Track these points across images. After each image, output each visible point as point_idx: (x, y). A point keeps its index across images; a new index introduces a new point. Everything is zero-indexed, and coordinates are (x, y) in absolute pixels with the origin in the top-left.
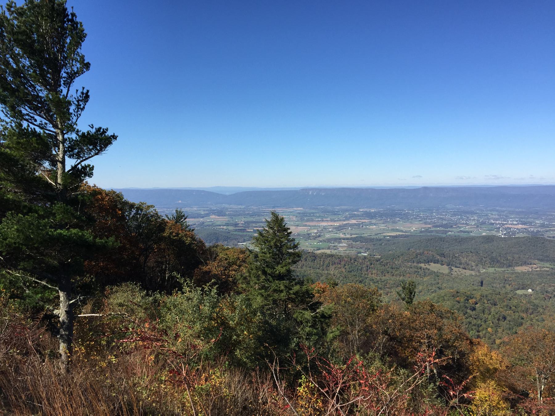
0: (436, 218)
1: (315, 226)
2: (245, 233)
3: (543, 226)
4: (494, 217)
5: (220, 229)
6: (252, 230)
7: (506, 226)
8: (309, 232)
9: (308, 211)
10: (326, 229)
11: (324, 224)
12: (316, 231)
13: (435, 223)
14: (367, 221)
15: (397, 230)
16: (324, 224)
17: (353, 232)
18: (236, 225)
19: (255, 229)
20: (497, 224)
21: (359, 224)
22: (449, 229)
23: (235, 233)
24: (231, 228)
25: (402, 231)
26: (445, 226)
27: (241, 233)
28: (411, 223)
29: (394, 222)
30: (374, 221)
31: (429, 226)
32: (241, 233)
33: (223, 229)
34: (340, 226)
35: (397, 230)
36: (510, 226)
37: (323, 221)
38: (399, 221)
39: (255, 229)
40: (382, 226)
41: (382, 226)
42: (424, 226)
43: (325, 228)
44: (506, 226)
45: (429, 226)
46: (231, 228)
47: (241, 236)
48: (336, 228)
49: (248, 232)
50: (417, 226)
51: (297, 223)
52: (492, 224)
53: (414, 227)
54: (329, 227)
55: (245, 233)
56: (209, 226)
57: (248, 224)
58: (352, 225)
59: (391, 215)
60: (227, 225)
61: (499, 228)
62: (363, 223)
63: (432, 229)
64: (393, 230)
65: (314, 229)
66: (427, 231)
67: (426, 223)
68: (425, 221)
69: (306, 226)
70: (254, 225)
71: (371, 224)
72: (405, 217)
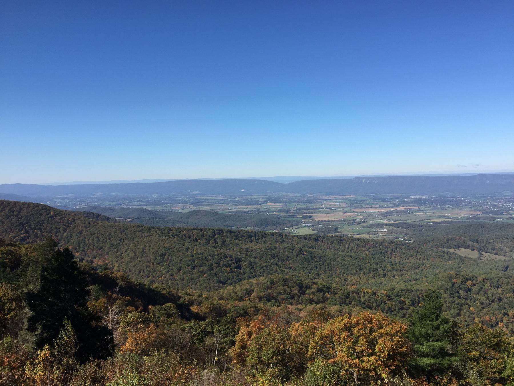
0: (489, 205)
1: (363, 212)
2: (294, 219)
5: (273, 215)
6: (301, 216)
8: (355, 218)
9: (359, 198)
10: (372, 215)
11: (372, 210)
12: (361, 217)
13: (485, 209)
14: (415, 208)
15: (444, 217)
16: (372, 210)
17: (399, 218)
18: (288, 211)
19: (305, 215)
21: (406, 211)
22: (499, 216)
23: (285, 219)
24: (283, 214)
25: (449, 218)
26: (496, 213)
27: (291, 219)
28: (461, 210)
30: (422, 208)
31: (479, 213)
32: (291, 219)
33: (275, 215)
34: (387, 213)
35: (444, 217)
37: (371, 208)
38: (449, 207)
39: (305, 215)
40: (430, 213)
41: (430, 213)
42: (473, 212)
43: (371, 214)
45: (479, 213)
46: (283, 214)
47: (290, 221)
48: (382, 214)
49: (298, 217)
50: (465, 213)
51: (345, 209)
53: (462, 214)
54: (376, 213)
55: (294, 219)
57: (299, 210)
58: (399, 212)
60: (280, 211)
62: (411, 209)
63: (481, 216)
64: (440, 217)
65: (361, 215)
66: (475, 217)
67: (476, 210)
68: (475, 208)
69: (354, 212)
70: (305, 211)
71: (419, 210)
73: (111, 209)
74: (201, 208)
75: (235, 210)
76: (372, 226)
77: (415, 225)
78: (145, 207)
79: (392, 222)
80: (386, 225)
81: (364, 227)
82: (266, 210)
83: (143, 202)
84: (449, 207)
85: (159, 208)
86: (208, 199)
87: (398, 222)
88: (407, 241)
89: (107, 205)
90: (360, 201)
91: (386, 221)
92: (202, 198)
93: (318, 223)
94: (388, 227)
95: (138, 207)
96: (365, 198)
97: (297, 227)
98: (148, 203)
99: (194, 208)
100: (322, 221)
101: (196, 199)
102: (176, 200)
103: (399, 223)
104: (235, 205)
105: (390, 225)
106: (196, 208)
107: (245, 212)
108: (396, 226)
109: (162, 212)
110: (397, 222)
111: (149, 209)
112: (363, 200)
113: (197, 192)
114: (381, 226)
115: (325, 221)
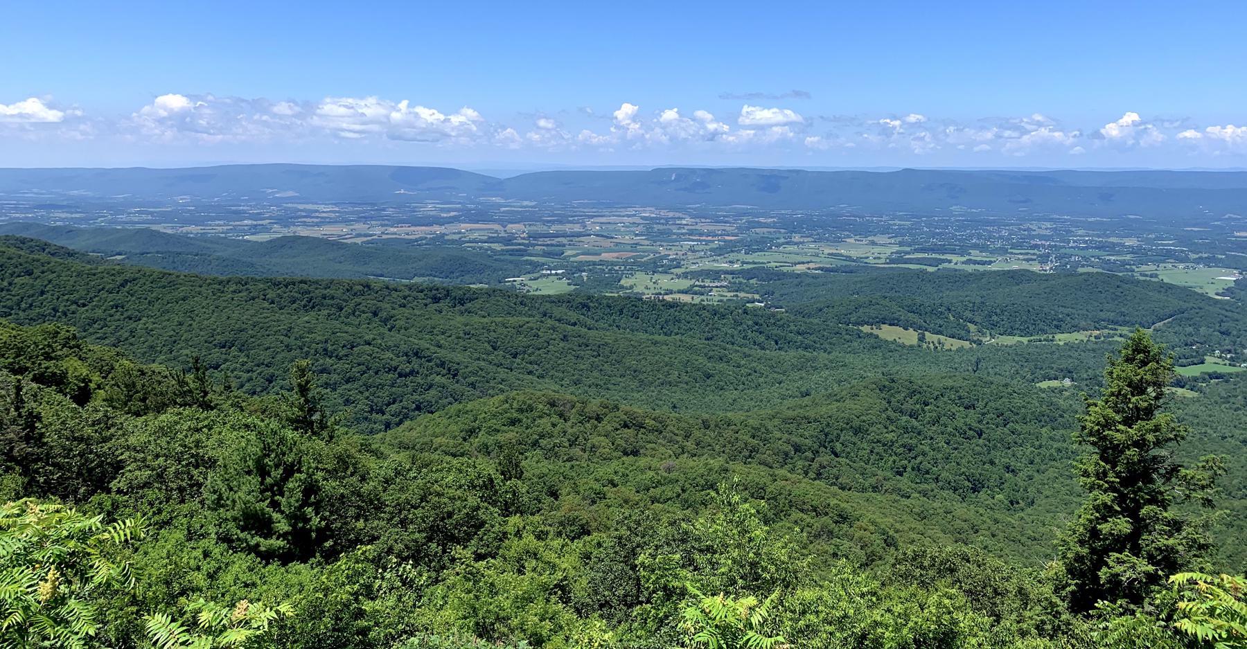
4: (1044, 232)
7: (1063, 251)
17: (749, 258)
18: (508, 241)
20: (1043, 246)
24: (497, 247)
29: (839, 240)
31: (908, 249)
33: (481, 248)
36: (1068, 251)
44: (1063, 251)
46: (497, 247)
52: (1036, 247)
56: (453, 241)
59: (831, 228)
60: (491, 240)
61: (1048, 255)
72: (863, 230)
73: (69, 232)
74: (303, 232)
75: (384, 237)
77: (784, 274)
78: (154, 227)
80: (726, 272)
81: (678, 277)
82: (456, 237)
83: (151, 213)
85: (193, 229)
86: (317, 211)
88: (772, 310)
89: (59, 218)
90: (667, 220)
92: (301, 207)
93: (580, 267)
94: (730, 277)
95: (138, 226)
96: (677, 215)
97: (532, 276)
98: (166, 218)
99: (279, 232)
100: (588, 263)
101: (286, 209)
102: (236, 212)
104: (382, 226)
106: (286, 230)
107: (409, 242)
108: (748, 274)
109: (203, 237)
111: (169, 231)
113: (290, 194)
114: (715, 275)
115: (594, 264)
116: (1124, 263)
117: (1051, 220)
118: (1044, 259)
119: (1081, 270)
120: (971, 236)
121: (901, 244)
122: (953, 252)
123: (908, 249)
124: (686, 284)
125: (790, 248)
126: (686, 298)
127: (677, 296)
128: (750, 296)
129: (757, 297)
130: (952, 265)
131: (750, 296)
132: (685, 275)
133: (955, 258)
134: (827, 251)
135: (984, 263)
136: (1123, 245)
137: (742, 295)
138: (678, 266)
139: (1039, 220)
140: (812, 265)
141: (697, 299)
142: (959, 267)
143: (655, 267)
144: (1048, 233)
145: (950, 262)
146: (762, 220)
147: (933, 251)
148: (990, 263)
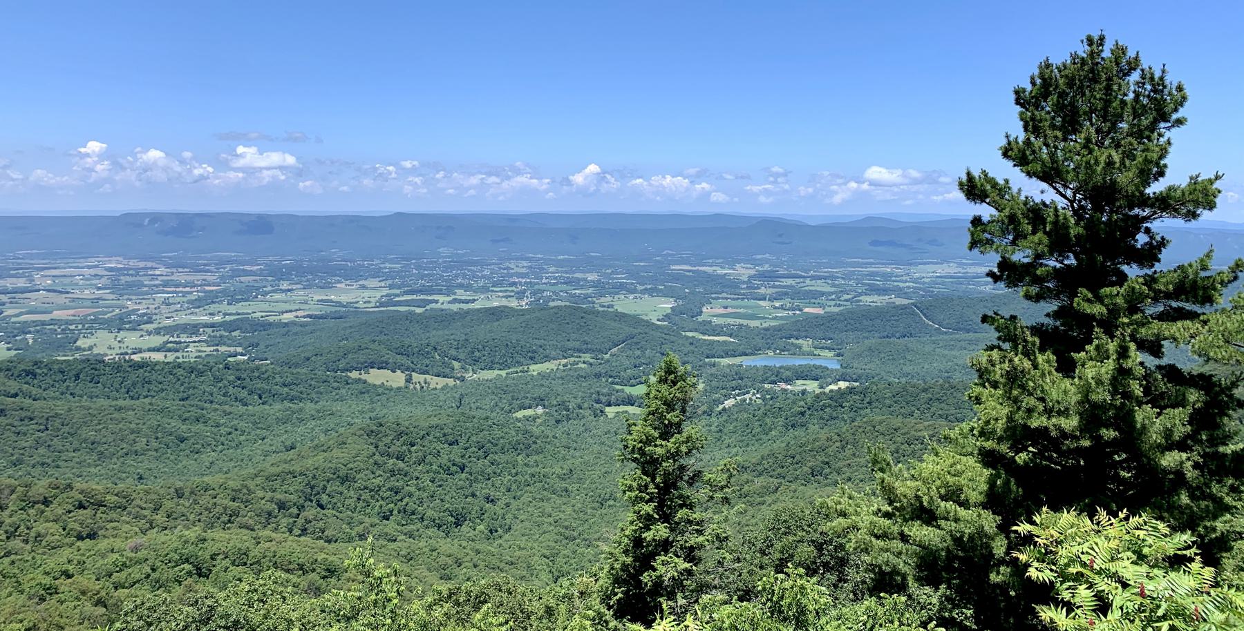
3: (595, 285)
7: (536, 287)
17: (232, 309)
22: (435, 297)
29: (327, 286)
31: (398, 291)
36: (541, 287)
44: (536, 287)
52: (514, 284)
59: (320, 273)
61: (524, 292)
76: (169, 330)
77: (270, 324)
79: (218, 318)
80: (206, 326)
81: (149, 333)
84: (339, 282)
87: (232, 318)
88: (257, 362)
90: (137, 270)
91: (205, 319)
93: (24, 329)
94: (209, 330)
96: (149, 264)
103: (235, 321)
105: (212, 326)
108: (230, 327)
110: (228, 318)
112: (145, 268)
114: (193, 329)
115: (43, 323)
116: (587, 296)
117: (526, 259)
118: (520, 295)
119: (552, 304)
120: (457, 276)
121: (391, 287)
122: (440, 292)
123: (398, 291)
124: (157, 340)
125: (277, 296)
126: (158, 357)
127: (146, 355)
128: (232, 349)
129: (239, 350)
130: (438, 306)
131: (232, 349)
132: (158, 332)
133: (441, 298)
134: (316, 298)
135: (467, 302)
136: (585, 279)
137: (223, 349)
138: (150, 322)
139: (517, 259)
140: (300, 313)
141: (171, 357)
142: (445, 306)
143: (120, 323)
144: (524, 270)
145: (437, 302)
146: (248, 268)
147: (420, 292)
148: (474, 301)
